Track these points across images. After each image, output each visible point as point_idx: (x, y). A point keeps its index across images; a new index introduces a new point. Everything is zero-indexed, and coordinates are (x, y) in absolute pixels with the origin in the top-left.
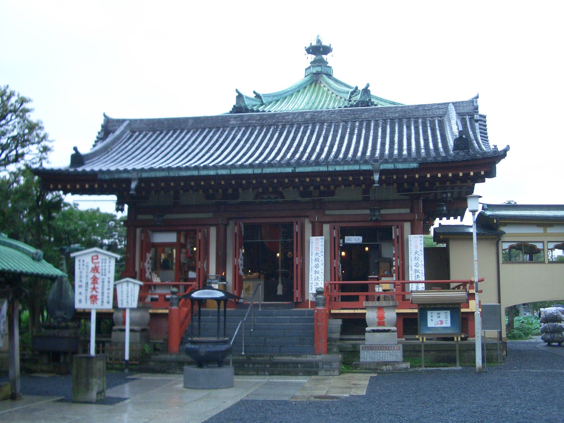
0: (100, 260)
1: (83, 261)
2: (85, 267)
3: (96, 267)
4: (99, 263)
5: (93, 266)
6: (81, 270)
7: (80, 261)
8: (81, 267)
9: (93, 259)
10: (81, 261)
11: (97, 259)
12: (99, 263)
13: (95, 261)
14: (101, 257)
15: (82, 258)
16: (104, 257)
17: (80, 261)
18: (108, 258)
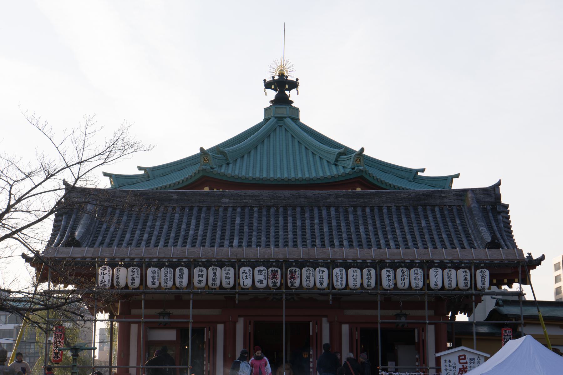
0: (467, 360)
1: (450, 361)
2: (452, 368)
3: (463, 368)
4: (466, 363)
5: (461, 366)
6: (448, 371)
7: (445, 361)
8: (448, 368)
9: (460, 360)
10: (447, 361)
11: (465, 359)
12: (466, 363)
13: (461, 361)
14: (468, 356)
15: (448, 358)
16: (472, 356)
17: (445, 361)
18: (476, 357)
